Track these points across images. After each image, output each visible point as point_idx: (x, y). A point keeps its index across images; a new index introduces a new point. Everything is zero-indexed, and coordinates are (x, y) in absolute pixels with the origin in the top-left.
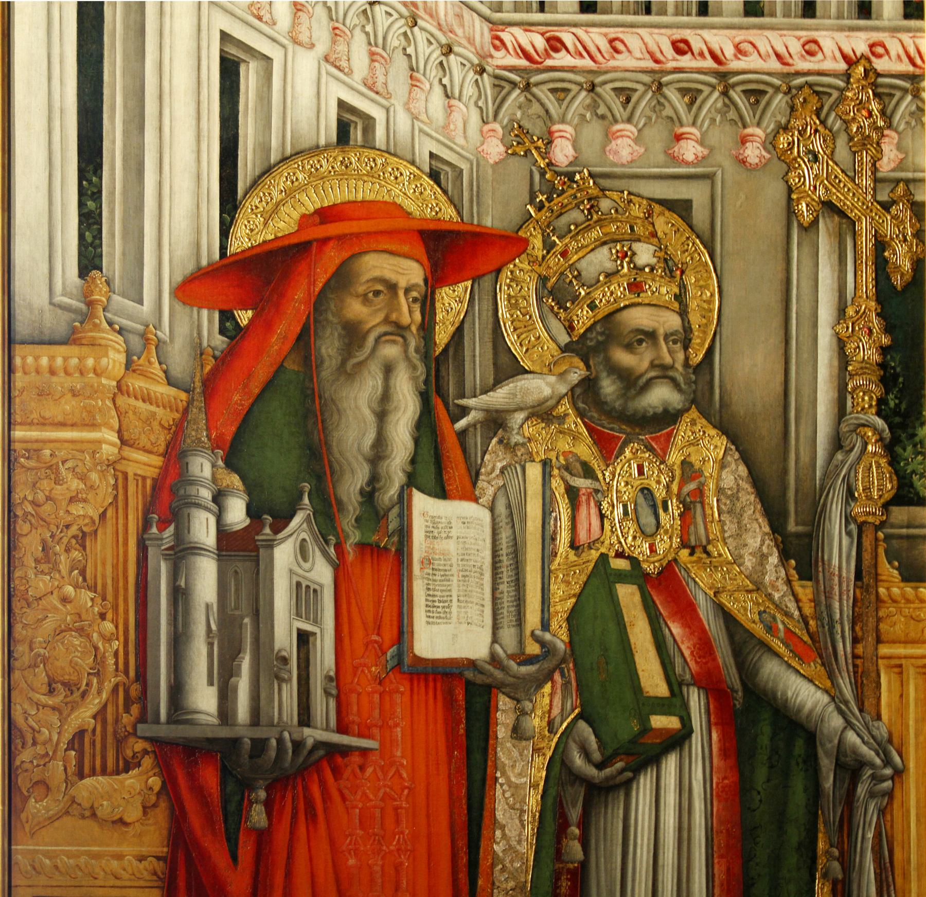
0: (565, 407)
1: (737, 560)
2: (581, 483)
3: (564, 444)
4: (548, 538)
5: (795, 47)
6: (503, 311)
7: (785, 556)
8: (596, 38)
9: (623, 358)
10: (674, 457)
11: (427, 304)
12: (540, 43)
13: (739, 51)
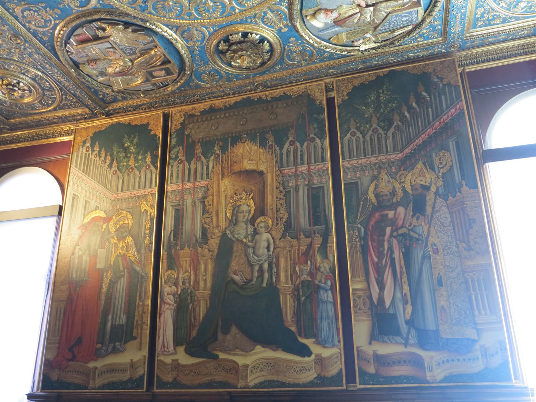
0: (115, 237)
1: (132, 253)
2: (116, 245)
3: (114, 241)
4: (112, 252)
5: (143, 192)
6: (110, 226)
7: (137, 251)
8: (122, 194)
9: (122, 230)
10: (126, 241)
11: (102, 227)
12: (117, 195)
13: (137, 193)
